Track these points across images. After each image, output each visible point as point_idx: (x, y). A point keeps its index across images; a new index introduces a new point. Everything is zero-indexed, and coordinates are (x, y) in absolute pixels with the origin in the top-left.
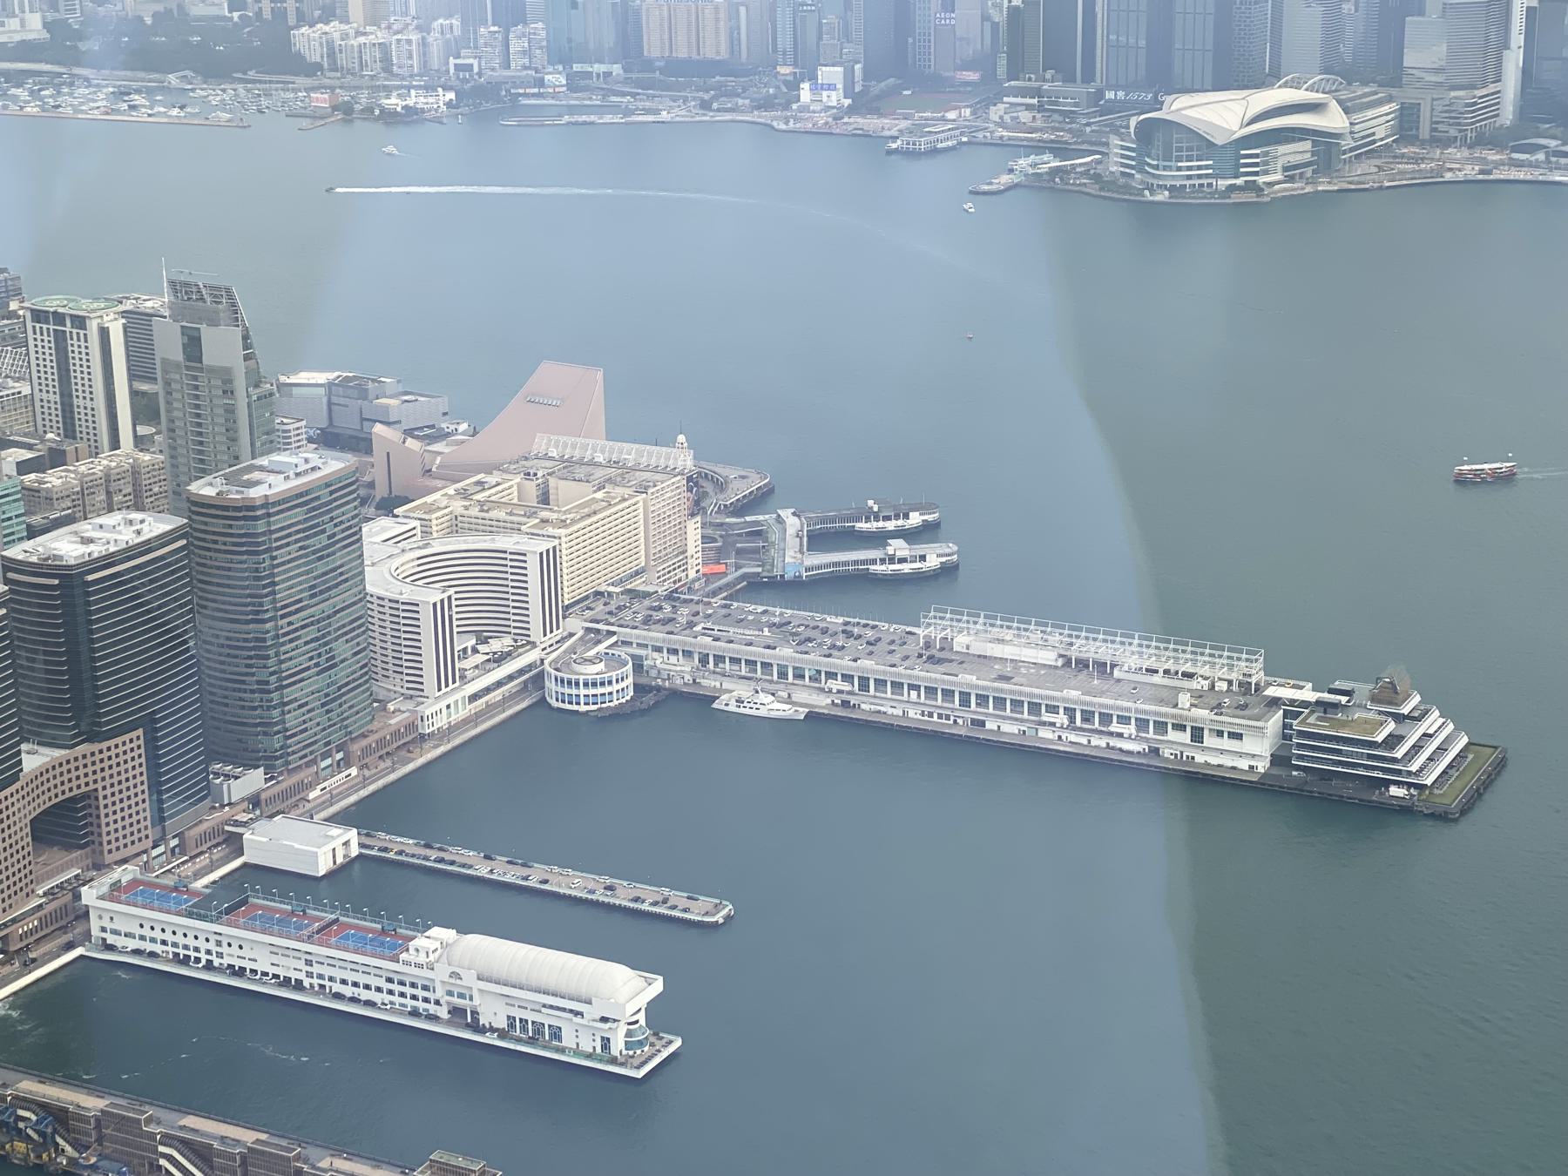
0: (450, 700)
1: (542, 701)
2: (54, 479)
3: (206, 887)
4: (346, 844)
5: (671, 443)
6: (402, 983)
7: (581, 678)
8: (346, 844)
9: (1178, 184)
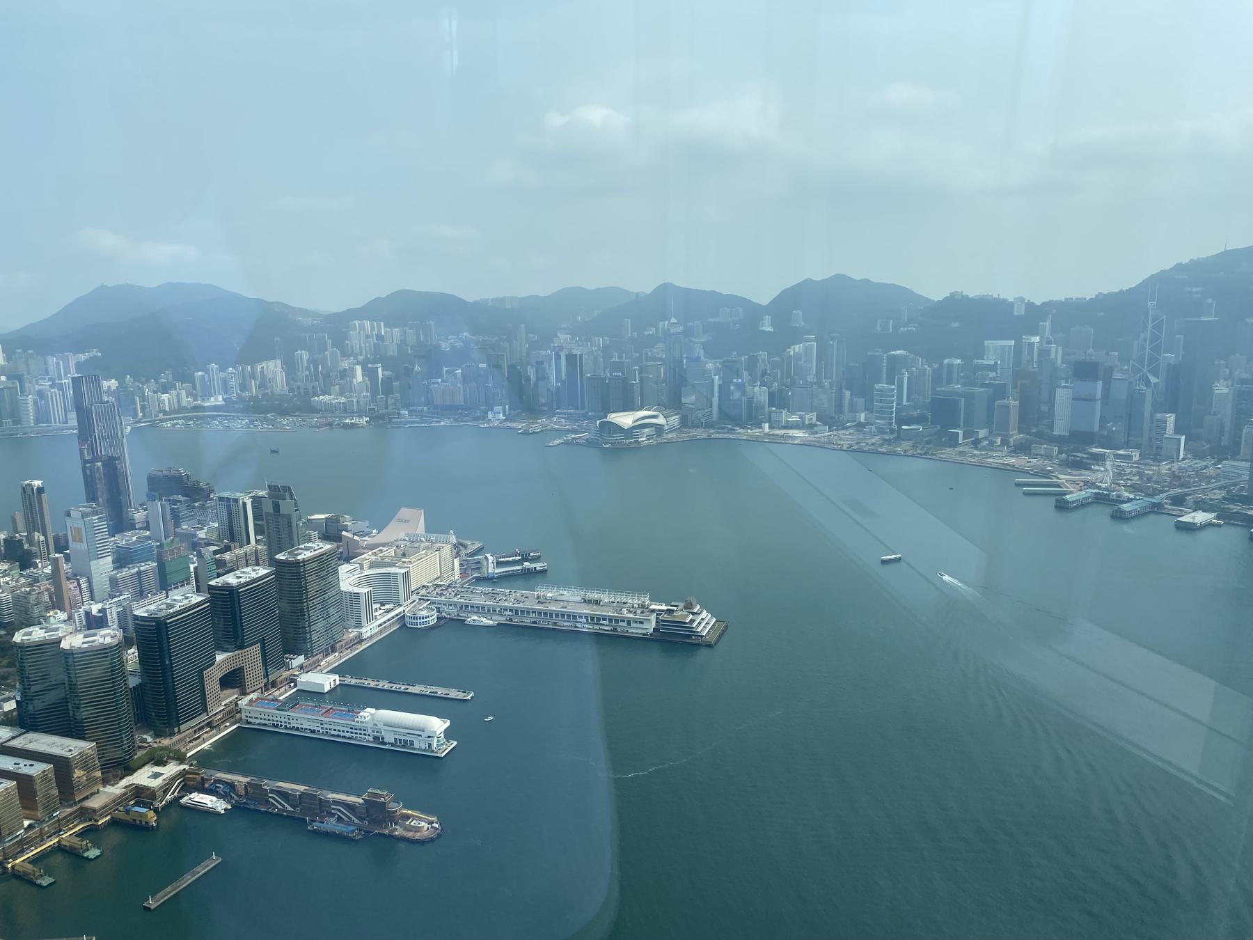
0: (371, 627)
2: (227, 556)
4: (335, 680)
5: (448, 533)
6: (356, 729)
8: (335, 680)
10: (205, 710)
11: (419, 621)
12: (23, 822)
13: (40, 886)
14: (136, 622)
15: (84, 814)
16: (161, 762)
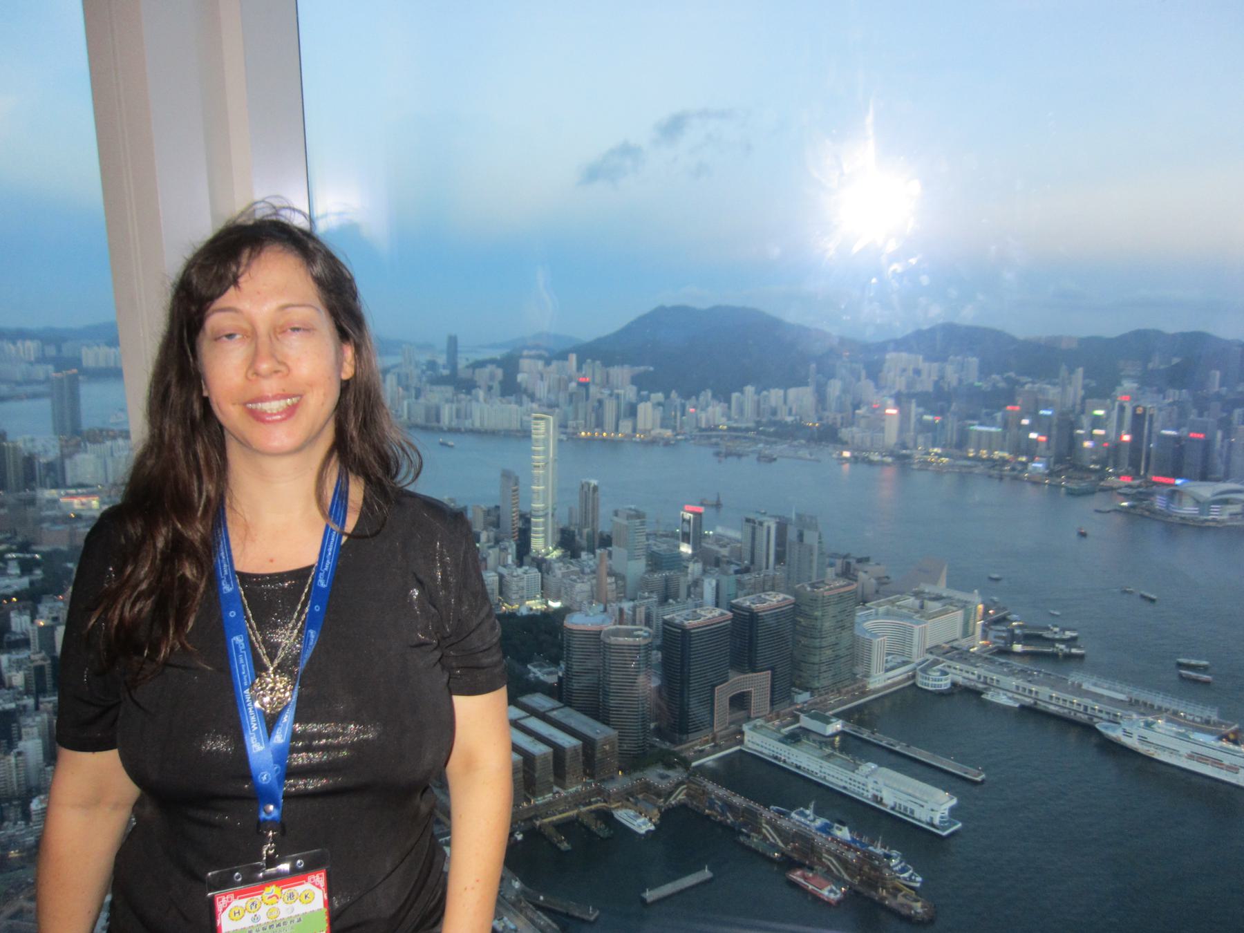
1: (914, 685)
2: (746, 577)
5: (970, 591)
6: (855, 781)
7: (931, 677)
9: (1183, 516)
10: (712, 726)
11: (930, 682)
13: (559, 849)
15: (599, 792)
16: (669, 766)
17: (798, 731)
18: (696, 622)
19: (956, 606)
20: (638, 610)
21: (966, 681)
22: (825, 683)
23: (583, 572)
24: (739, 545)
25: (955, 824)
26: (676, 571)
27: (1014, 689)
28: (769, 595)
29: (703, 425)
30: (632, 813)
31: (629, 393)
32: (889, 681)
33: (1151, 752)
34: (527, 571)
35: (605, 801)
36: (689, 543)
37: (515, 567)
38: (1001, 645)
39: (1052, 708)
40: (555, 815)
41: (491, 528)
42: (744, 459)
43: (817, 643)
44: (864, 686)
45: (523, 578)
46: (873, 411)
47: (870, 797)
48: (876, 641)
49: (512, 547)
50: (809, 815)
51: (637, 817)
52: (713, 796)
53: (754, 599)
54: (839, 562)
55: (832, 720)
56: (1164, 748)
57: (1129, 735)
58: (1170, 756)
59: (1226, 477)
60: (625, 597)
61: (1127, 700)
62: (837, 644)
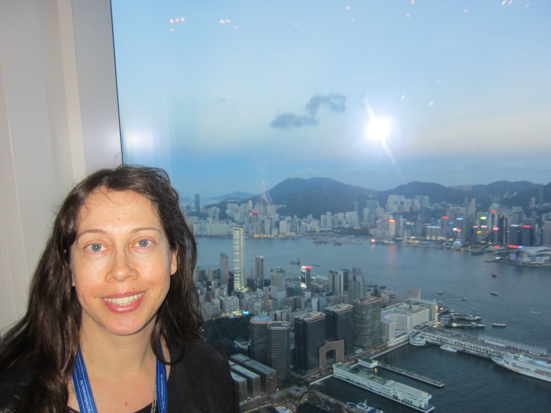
1: (409, 344)
2: (331, 297)
3: (353, 367)
5: (432, 300)
6: (384, 389)
9: (524, 262)
10: (319, 365)
11: (416, 342)
12: (247, 397)
14: (297, 321)
15: (269, 398)
16: (300, 385)
17: (357, 367)
18: (309, 318)
19: (425, 307)
20: (283, 314)
21: (432, 341)
22: (369, 344)
23: (258, 298)
24: (327, 283)
25: (431, 407)
26: (299, 296)
27: (454, 344)
28: (342, 305)
29: (309, 230)
30: (284, 408)
31: (276, 217)
32: (398, 342)
33: (518, 370)
34: (233, 298)
35: (271, 403)
36: (305, 283)
37: (227, 296)
38: (447, 324)
39: (472, 352)
40: (249, 410)
41: (216, 279)
42: (327, 244)
43: (364, 326)
44: (387, 345)
45: (231, 301)
46: (384, 221)
47: (392, 396)
48: (391, 324)
49: (226, 287)
50: (364, 406)
51: (286, 410)
52: (320, 399)
53: (335, 307)
54: (372, 289)
55: (373, 361)
56: (523, 368)
57: (507, 363)
58: (527, 372)
59: (541, 244)
60: (277, 308)
61: (505, 346)
62: (373, 326)
